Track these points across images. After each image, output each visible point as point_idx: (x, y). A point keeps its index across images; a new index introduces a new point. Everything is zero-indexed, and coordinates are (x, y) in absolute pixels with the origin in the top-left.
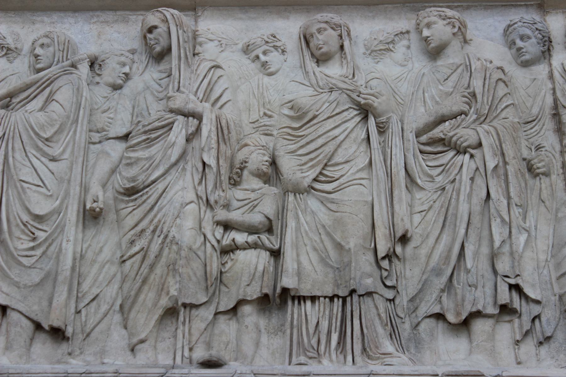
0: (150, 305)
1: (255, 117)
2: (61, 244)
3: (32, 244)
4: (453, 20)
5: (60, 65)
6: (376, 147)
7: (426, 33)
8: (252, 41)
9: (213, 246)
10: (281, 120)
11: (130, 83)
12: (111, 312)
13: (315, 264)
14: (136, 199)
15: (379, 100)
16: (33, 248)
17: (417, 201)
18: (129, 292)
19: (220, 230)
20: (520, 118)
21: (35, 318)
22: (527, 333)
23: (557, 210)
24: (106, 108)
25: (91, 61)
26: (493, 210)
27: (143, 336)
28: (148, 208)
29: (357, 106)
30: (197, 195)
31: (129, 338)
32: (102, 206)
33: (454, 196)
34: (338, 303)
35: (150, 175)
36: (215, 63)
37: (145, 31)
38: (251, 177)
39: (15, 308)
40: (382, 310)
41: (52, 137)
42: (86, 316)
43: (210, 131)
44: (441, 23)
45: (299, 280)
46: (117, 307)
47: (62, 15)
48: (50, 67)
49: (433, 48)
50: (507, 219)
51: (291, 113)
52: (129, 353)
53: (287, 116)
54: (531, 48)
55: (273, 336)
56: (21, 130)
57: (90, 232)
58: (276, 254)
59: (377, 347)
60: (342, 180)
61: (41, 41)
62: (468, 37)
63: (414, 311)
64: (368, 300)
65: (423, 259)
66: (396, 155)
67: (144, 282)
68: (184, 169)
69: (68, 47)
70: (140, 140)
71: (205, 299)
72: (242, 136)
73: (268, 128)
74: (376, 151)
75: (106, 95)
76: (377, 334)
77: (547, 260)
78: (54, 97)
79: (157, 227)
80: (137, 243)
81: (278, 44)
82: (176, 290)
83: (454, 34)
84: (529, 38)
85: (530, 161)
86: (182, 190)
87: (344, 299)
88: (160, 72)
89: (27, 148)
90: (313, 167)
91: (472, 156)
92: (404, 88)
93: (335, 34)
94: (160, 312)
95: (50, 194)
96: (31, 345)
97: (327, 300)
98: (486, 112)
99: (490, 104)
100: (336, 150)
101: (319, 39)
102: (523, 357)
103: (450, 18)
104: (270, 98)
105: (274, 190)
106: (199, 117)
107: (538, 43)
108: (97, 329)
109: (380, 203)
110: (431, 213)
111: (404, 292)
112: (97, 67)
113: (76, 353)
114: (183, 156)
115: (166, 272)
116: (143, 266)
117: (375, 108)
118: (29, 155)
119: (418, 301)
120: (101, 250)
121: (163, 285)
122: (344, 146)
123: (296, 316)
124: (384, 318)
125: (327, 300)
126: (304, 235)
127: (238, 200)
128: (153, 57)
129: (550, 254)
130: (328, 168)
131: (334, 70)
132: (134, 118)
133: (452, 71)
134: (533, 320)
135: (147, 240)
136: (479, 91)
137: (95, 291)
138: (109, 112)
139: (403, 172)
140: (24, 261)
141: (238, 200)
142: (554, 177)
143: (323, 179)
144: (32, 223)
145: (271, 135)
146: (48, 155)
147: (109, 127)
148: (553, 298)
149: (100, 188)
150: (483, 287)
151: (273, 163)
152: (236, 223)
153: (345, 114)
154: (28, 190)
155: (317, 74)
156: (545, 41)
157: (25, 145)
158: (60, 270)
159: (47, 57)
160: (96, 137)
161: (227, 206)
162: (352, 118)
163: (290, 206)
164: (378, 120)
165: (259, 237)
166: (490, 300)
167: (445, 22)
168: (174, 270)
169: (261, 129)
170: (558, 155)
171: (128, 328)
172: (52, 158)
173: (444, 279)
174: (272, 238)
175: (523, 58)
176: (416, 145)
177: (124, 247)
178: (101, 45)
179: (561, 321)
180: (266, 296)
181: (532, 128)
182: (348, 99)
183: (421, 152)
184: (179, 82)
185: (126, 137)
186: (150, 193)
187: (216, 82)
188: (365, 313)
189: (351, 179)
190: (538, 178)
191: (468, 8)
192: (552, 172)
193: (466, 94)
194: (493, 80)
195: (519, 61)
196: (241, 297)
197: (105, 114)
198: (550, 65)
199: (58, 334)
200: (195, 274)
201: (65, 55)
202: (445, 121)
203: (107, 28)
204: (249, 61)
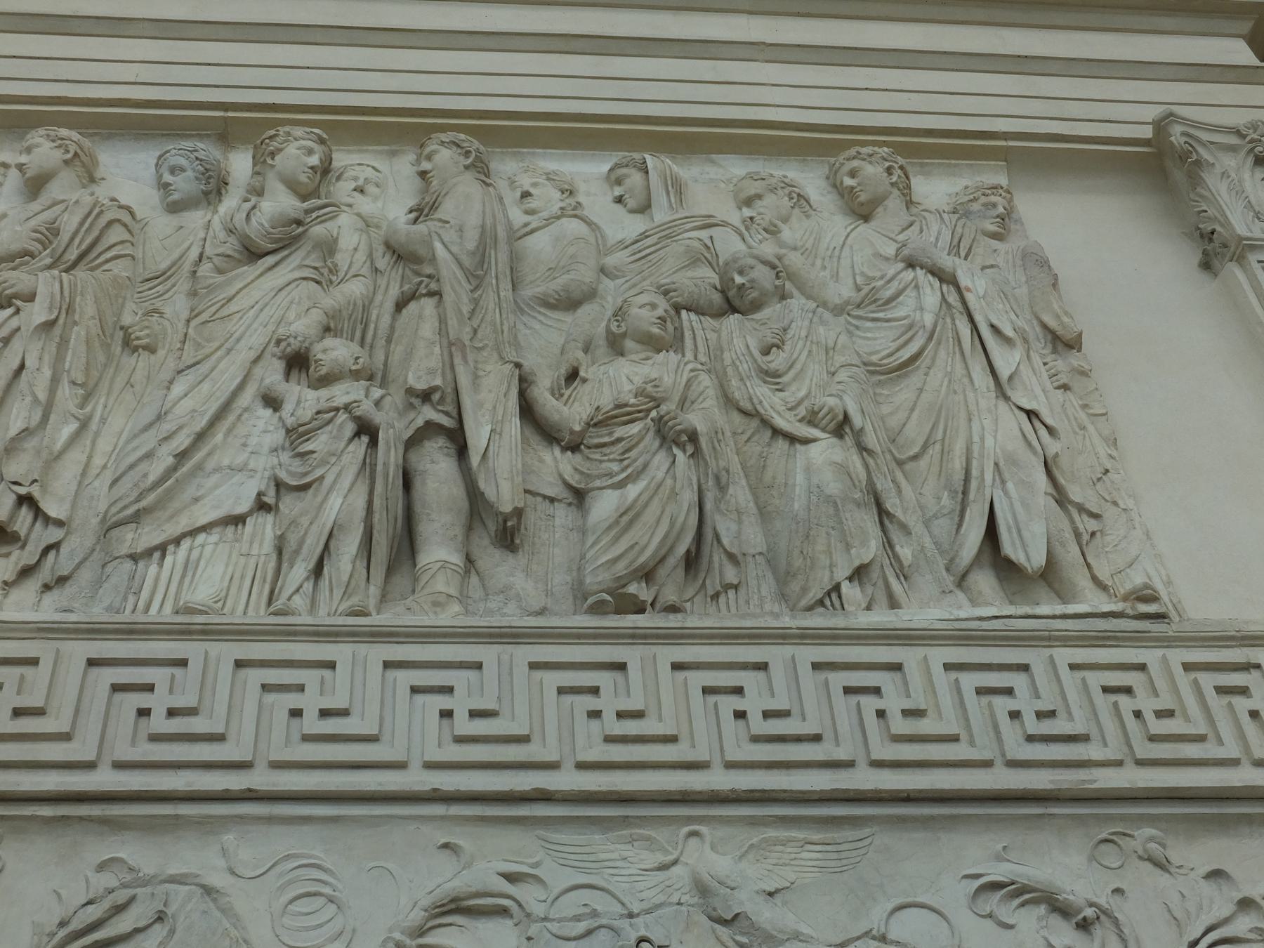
22: (26, 572)
50: (42, 396)
54: (184, 184)
62: (98, 175)
83: (66, 162)
84: (183, 170)
99: (83, 247)
103: (62, 139)
142: (161, 353)
156: (210, 177)
170: (181, 326)
175: (171, 198)
179: (95, 553)
181: (150, 289)
191: (109, 137)
192: (160, 345)
194: (103, 221)
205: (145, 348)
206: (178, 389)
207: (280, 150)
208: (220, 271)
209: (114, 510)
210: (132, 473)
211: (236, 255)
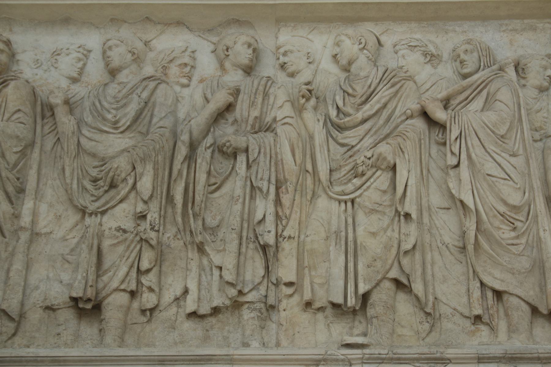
2: (538, 233)
5: (487, 70)
16: (517, 237)
21: (533, 303)
24: (539, 108)
39: (514, 293)
41: (506, 134)
47: (473, 23)
56: (476, 128)
61: (464, 47)
75: (535, 96)
89: (486, 145)
95: (519, 186)
96: (531, 328)
112: (520, 72)
144: (509, 213)
147: (546, 126)
154: (497, 184)
157: (483, 142)
158: (545, 258)
159: (473, 62)
172: (512, 153)
178: (515, 51)
197: (539, 114)
201: (488, 60)
203: (517, 36)
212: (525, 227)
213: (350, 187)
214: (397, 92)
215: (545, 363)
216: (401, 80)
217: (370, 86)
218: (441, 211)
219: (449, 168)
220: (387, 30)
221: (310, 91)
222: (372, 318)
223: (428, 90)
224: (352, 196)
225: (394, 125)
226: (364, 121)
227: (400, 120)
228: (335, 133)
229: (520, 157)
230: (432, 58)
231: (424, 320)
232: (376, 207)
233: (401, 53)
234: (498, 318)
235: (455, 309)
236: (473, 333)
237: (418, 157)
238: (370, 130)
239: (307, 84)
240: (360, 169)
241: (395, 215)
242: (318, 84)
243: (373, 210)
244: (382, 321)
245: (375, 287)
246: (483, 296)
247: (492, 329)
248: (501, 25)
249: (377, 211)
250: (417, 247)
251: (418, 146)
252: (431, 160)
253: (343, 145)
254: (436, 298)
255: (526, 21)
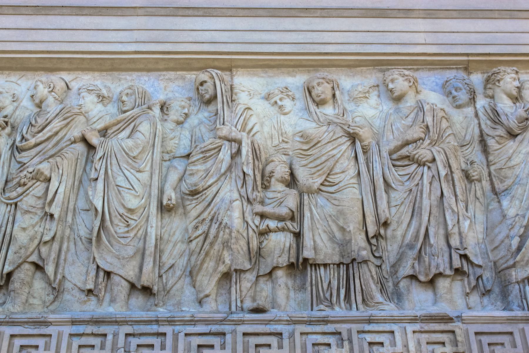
0: (211, 271)
1: (276, 142)
2: (146, 230)
3: (126, 229)
4: (409, 77)
5: (140, 107)
6: (362, 162)
7: (391, 86)
8: (272, 92)
9: (253, 230)
10: (296, 144)
11: (189, 120)
12: (183, 276)
13: (325, 242)
14: (198, 198)
15: (363, 130)
16: (128, 232)
17: (392, 199)
18: (196, 262)
19: (257, 220)
20: (458, 143)
21: (131, 280)
23: (488, 205)
25: (161, 105)
26: (446, 204)
27: (207, 292)
28: (207, 204)
29: (347, 134)
30: (240, 195)
31: (197, 295)
32: (174, 203)
33: (419, 195)
34: (343, 269)
35: (207, 181)
36: (246, 106)
37: (197, 84)
38: (277, 183)
40: (374, 273)
41: (137, 156)
42: (166, 279)
43: (248, 151)
44: (401, 79)
45: (315, 252)
46: (188, 273)
48: (133, 109)
49: (396, 96)
50: (456, 210)
51: (302, 140)
52: (197, 304)
53: (299, 142)
54: (463, 96)
55: (297, 292)
56: (116, 151)
57: (166, 220)
58: (298, 236)
59: (372, 299)
60: (341, 185)
61: (126, 91)
63: (395, 274)
64: (364, 266)
65: (399, 238)
66: (376, 167)
67: (207, 254)
68: (231, 178)
69: (144, 95)
70: (198, 157)
71: (249, 267)
72: (268, 156)
73: (286, 150)
74: (363, 165)
75: (172, 128)
76: (371, 289)
77: (483, 239)
78: (138, 129)
79: (213, 217)
80: (200, 228)
81: (290, 93)
82: (230, 260)
83: (410, 87)
84: (461, 89)
85: (467, 171)
86: (229, 191)
87: (348, 265)
88: (210, 112)
90: (320, 175)
91: (429, 168)
92: (377, 123)
93: (329, 86)
94: (219, 275)
96: (128, 299)
97: (335, 266)
98: (436, 138)
100: (335, 164)
101: (317, 91)
102: (472, 304)
103: (407, 76)
104: (286, 130)
105: (294, 192)
106: (240, 143)
107: (467, 93)
108: (174, 288)
109: (368, 200)
110: (403, 207)
111: (387, 261)
112: (165, 110)
113: (160, 305)
114: (229, 169)
115: (222, 248)
116: (206, 244)
117: (360, 136)
118: (122, 168)
119: (397, 266)
120: (174, 234)
121: (220, 257)
122: (341, 161)
123: (314, 278)
124: (376, 278)
125: (335, 266)
126: (316, 222)
127: (269, 199)
128: (203, 102)
129: (485, 234)
130: (330, 177)
131: (329, 110)
132: (193, 143)
133: (410, 112)
134: (478, 279)
135: (207, 226)
136: (430, 124)
137: (171, 262)
138: (175, 139)
139: (382, 180)
140: (122, 241)
141: (269, 199)
142: (484, 182)
143: (328, 184)
144: (126, 214)
145: (288, 155)
146: (136, 168)
148: (489, 264)
149: (173, 190)
150: (443, 256)
151: (292, 174)
152: (270, 213)
153: (340, 140)
154: (122, 192)
155: (318, 113)
156: (472, 92)
160: (167, 157)
161: (262, 203)
162: (345, 143)
163: (306, 202)
164: (363, 144)
165: (285, 224)
166: (448, 265)
167: (404, 79)
168: (228, 246)
169: (280, 151)
170: (485, 168)
171: (196, 287)
173: (416, 251)
174: (295, 225)
175: (458, 103)
176: (390, 161)
177: (190, 231)
178: (167, 95)
180: (292, 264)
181: (466, 150)
182: (341, 130)
183: (394, 166)
184: (224, 119)
185: (188, 156)
186: (207, 194)
187: (249, 118)
188: (363, 275)
189: (346, 183)
190: (473, 183)
193: (422, 126)
194: (439, 118)
195: (454, 105)
196: (275, 265)
197: (172, 141)
198: (475, 108)
199: (147, 290)
200: (242, 249)
201: (143, 101)
202: (408, 144)
203: (171, 83)
204: (269, 105)
205: (476, 180)
206: (505, 203)
207: (502, 79)
208: (500, 144)
209: (501, 261)
210: (503, 244)
211: (505, 136)
212: (135, 225)
213: (14, 194)
214: (68, 123)
215: (121, 325)
216: (73, 115)
217: (47, 119)
218: (82, 212)
219: (92, 181)
220: (76, 78)
221: (6, 123)
222: (10, 291)
223: (95, 122)
224: (15, 201)
225: (59, 148)
226: (37, 145)
227: (65, 145)
228: (16, 153)
229: (146, 172)
230: (102, 98)
231: (51, 293)
232: (30, 209)
233: (82, 95)
234: (105, 291)
235: (75, 285)
236: (85, 302)
237: (73, 171)
238: (40, 152)
239: (6, 117)
240: (22, 181)
241: (45, 215)
242: (15, 117)
243: (27, 211)
244: (18, 293)
245: (17, 268)
246: (97, 276)
247: (99, 300)
248: (160, 75)
249: (30, 212)
250: (56, 239)
251: (74, 164)
252: (84, 173)
253: (19, 163)
254: (64, 277)
255: (178, 73)
